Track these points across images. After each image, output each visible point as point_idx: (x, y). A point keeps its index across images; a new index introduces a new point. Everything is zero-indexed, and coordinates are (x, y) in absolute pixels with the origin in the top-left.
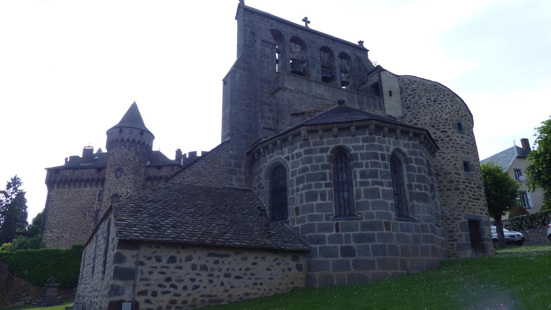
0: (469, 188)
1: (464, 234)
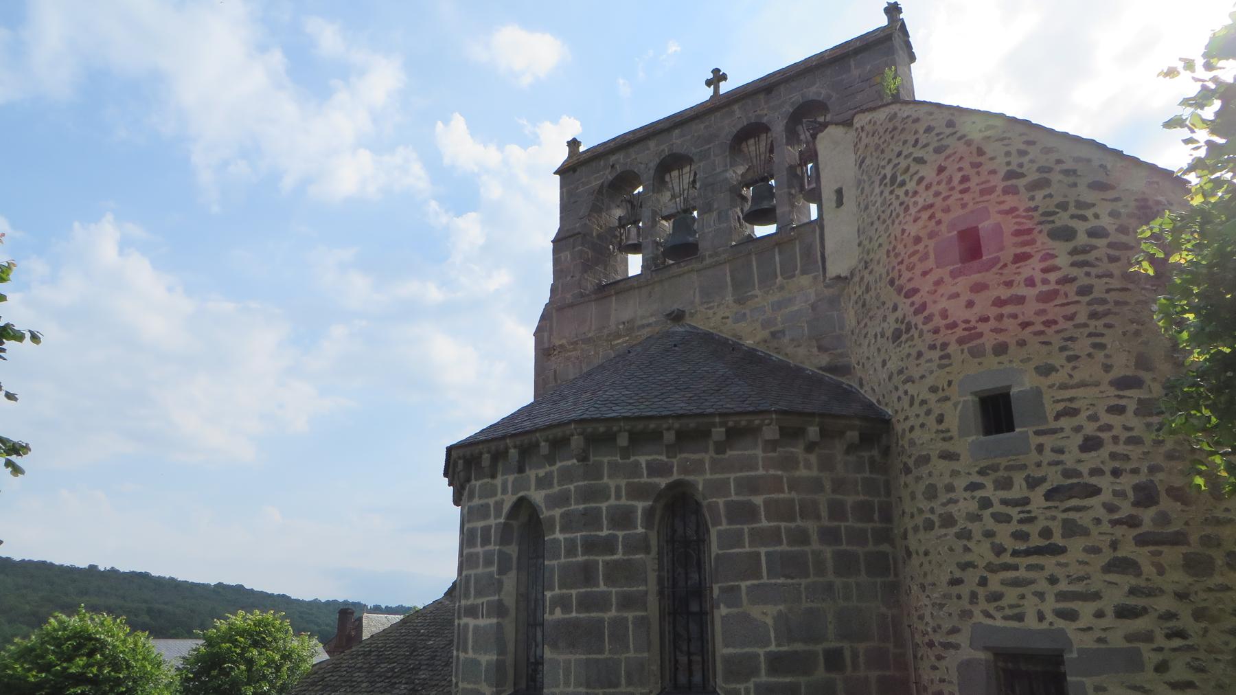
0: (998, 508)
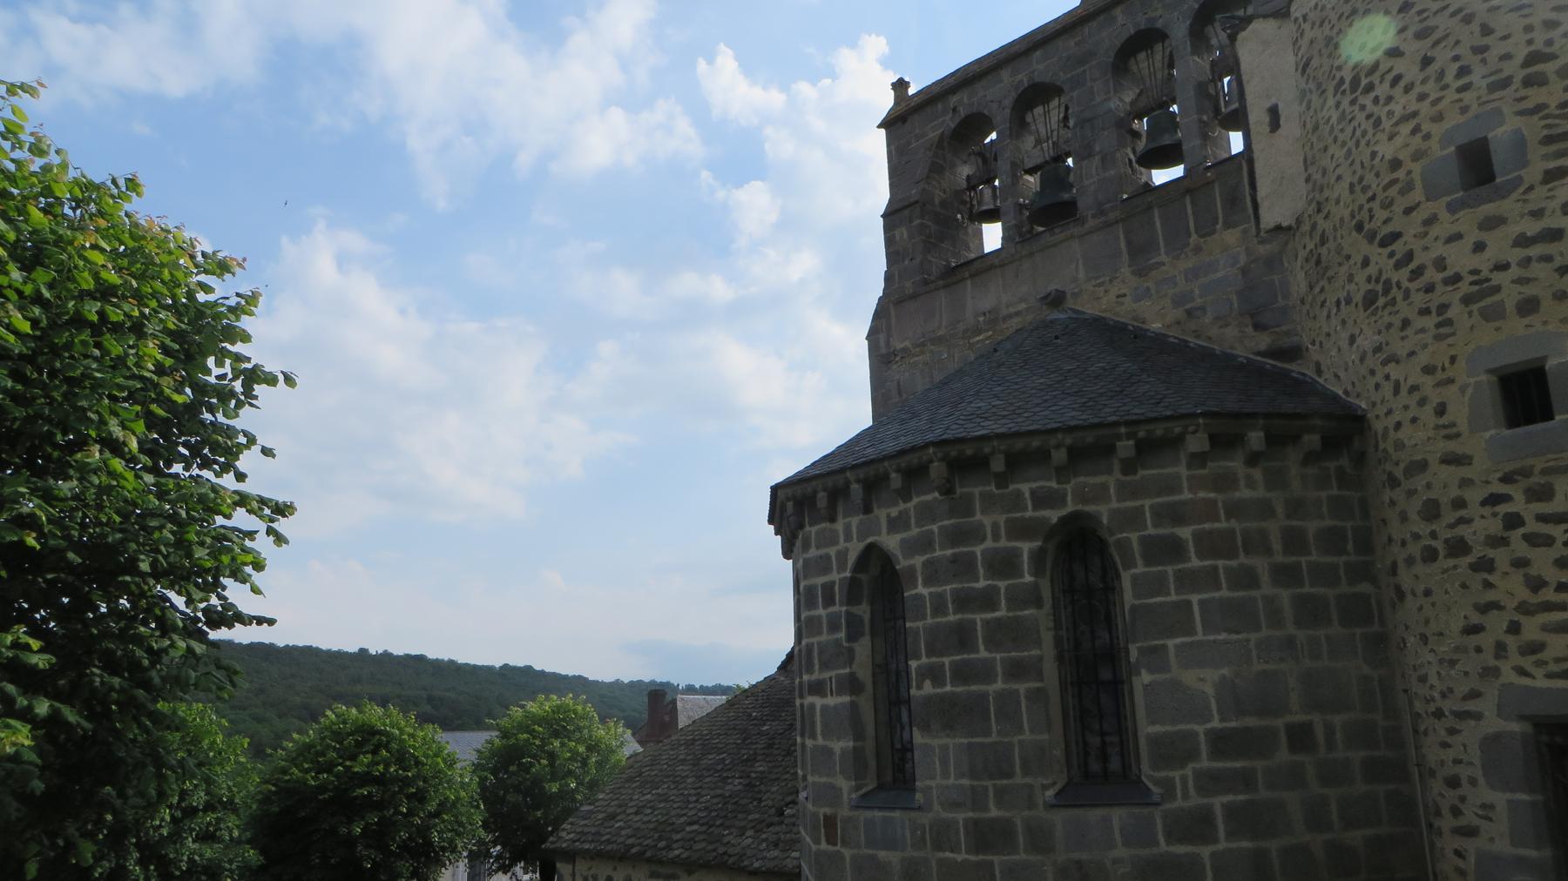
0: (1532, 526)
1: (1500, 799)
